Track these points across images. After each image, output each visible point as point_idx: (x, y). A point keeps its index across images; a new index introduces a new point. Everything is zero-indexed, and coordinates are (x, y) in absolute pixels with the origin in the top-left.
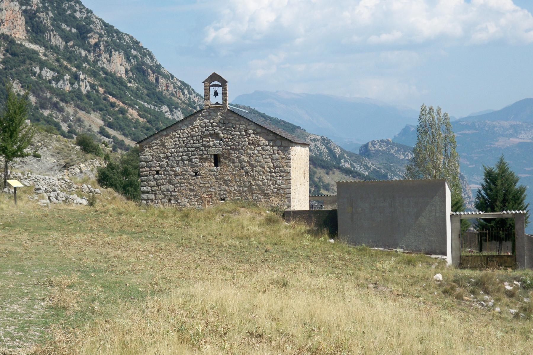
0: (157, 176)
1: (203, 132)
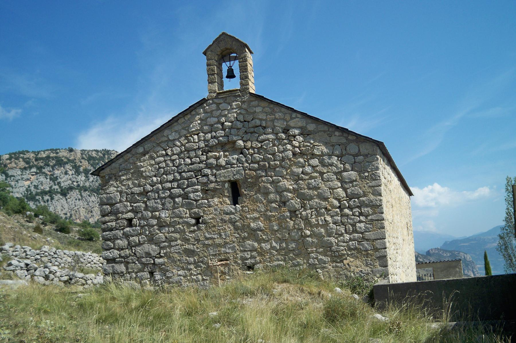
0: (128, 229)
1: (208, 141)
